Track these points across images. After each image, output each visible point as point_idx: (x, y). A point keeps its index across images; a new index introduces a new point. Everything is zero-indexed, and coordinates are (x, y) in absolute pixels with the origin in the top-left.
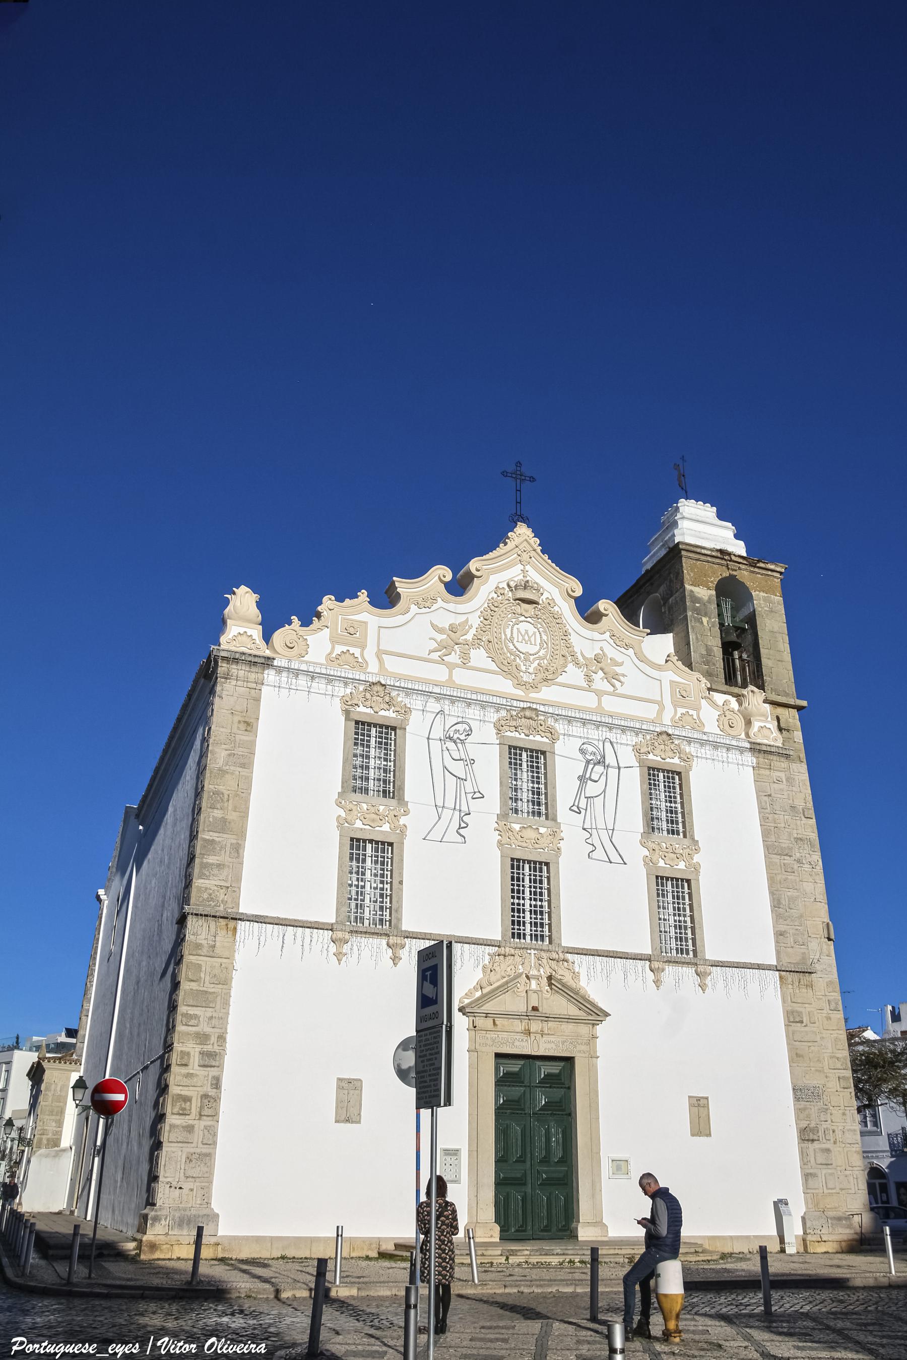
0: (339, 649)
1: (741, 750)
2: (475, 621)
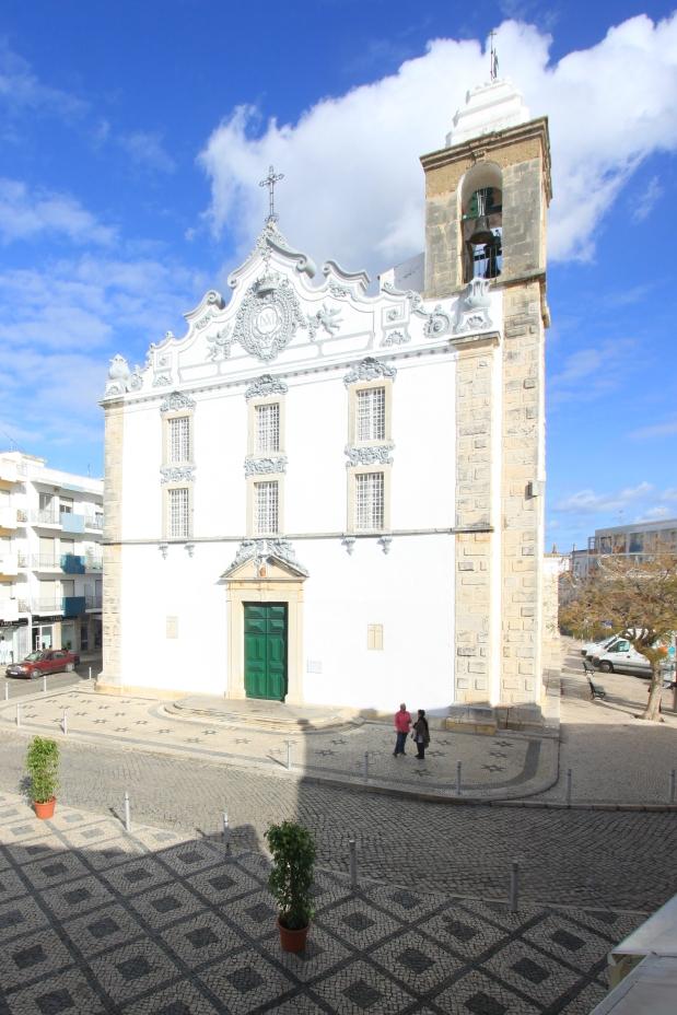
0: (159, 376)
1: (446, 350)
2: (233, 322)
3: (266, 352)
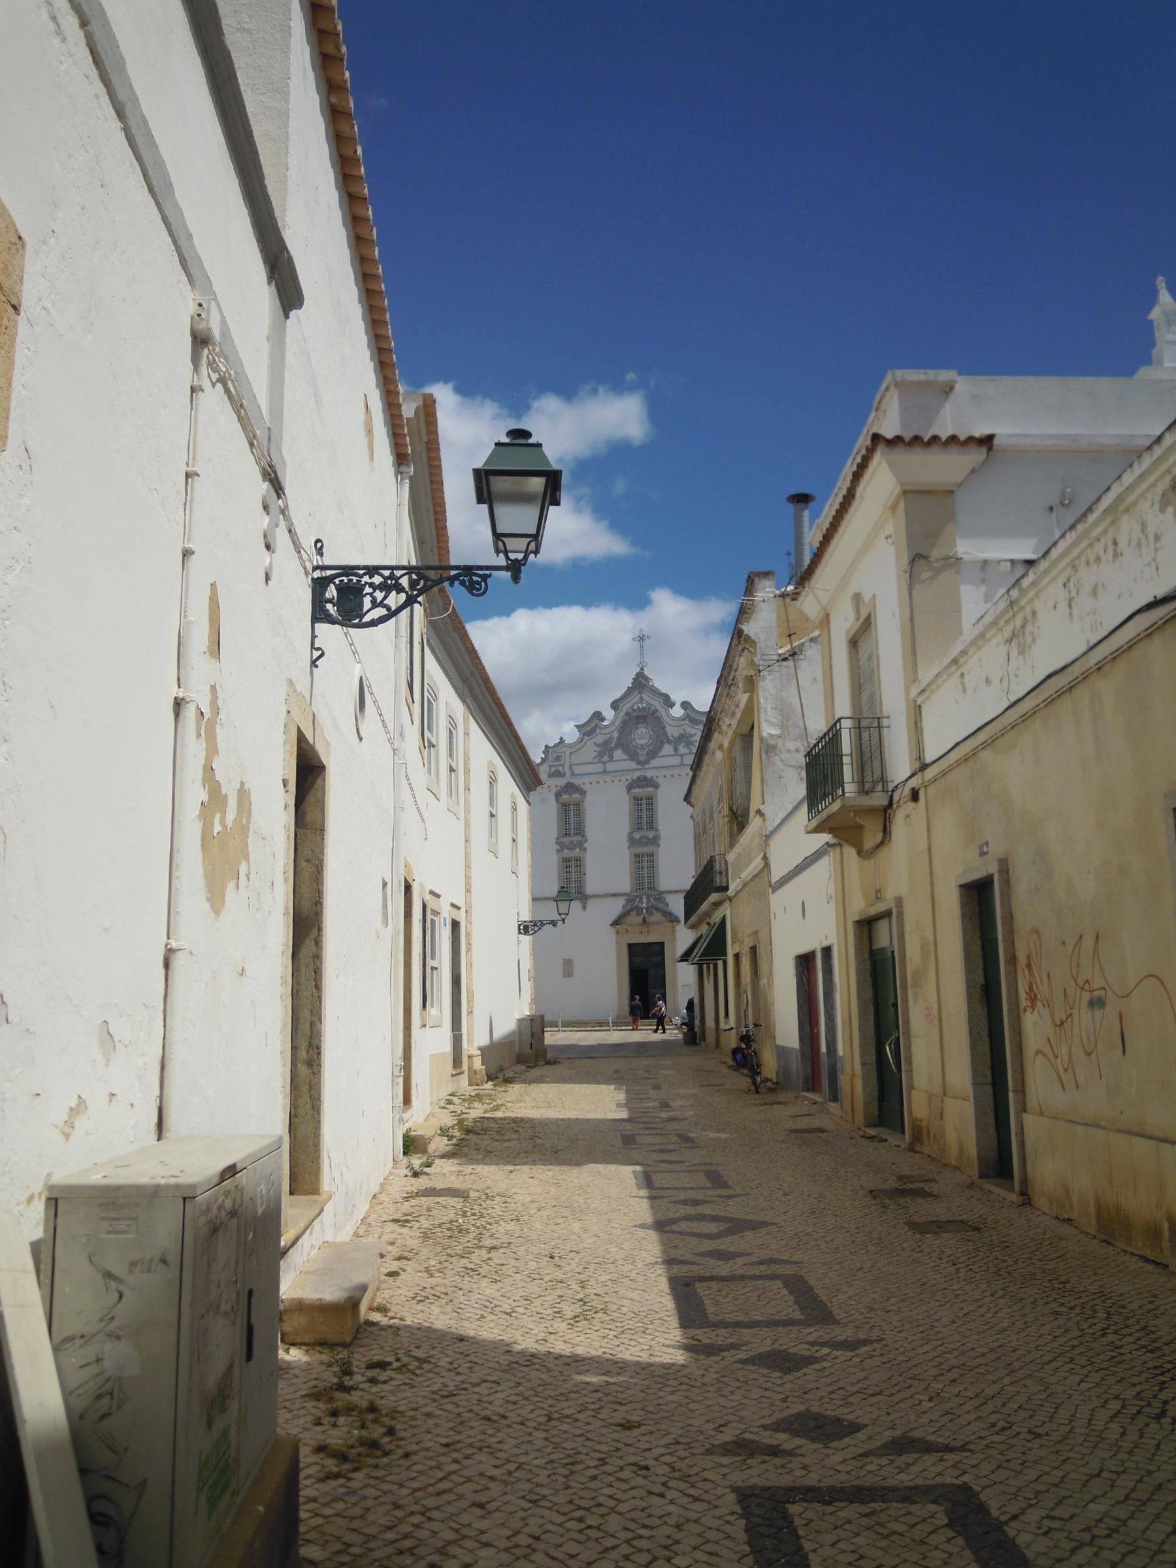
0: (553, 769)
2: (616, 735)
3: (642, 758)
